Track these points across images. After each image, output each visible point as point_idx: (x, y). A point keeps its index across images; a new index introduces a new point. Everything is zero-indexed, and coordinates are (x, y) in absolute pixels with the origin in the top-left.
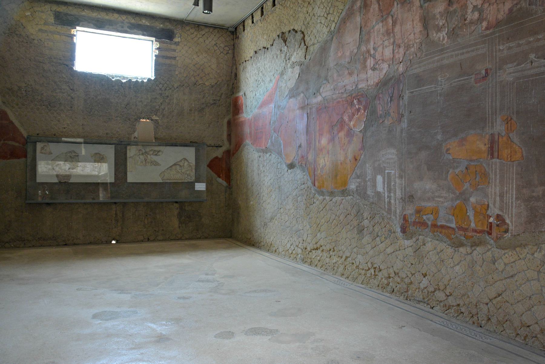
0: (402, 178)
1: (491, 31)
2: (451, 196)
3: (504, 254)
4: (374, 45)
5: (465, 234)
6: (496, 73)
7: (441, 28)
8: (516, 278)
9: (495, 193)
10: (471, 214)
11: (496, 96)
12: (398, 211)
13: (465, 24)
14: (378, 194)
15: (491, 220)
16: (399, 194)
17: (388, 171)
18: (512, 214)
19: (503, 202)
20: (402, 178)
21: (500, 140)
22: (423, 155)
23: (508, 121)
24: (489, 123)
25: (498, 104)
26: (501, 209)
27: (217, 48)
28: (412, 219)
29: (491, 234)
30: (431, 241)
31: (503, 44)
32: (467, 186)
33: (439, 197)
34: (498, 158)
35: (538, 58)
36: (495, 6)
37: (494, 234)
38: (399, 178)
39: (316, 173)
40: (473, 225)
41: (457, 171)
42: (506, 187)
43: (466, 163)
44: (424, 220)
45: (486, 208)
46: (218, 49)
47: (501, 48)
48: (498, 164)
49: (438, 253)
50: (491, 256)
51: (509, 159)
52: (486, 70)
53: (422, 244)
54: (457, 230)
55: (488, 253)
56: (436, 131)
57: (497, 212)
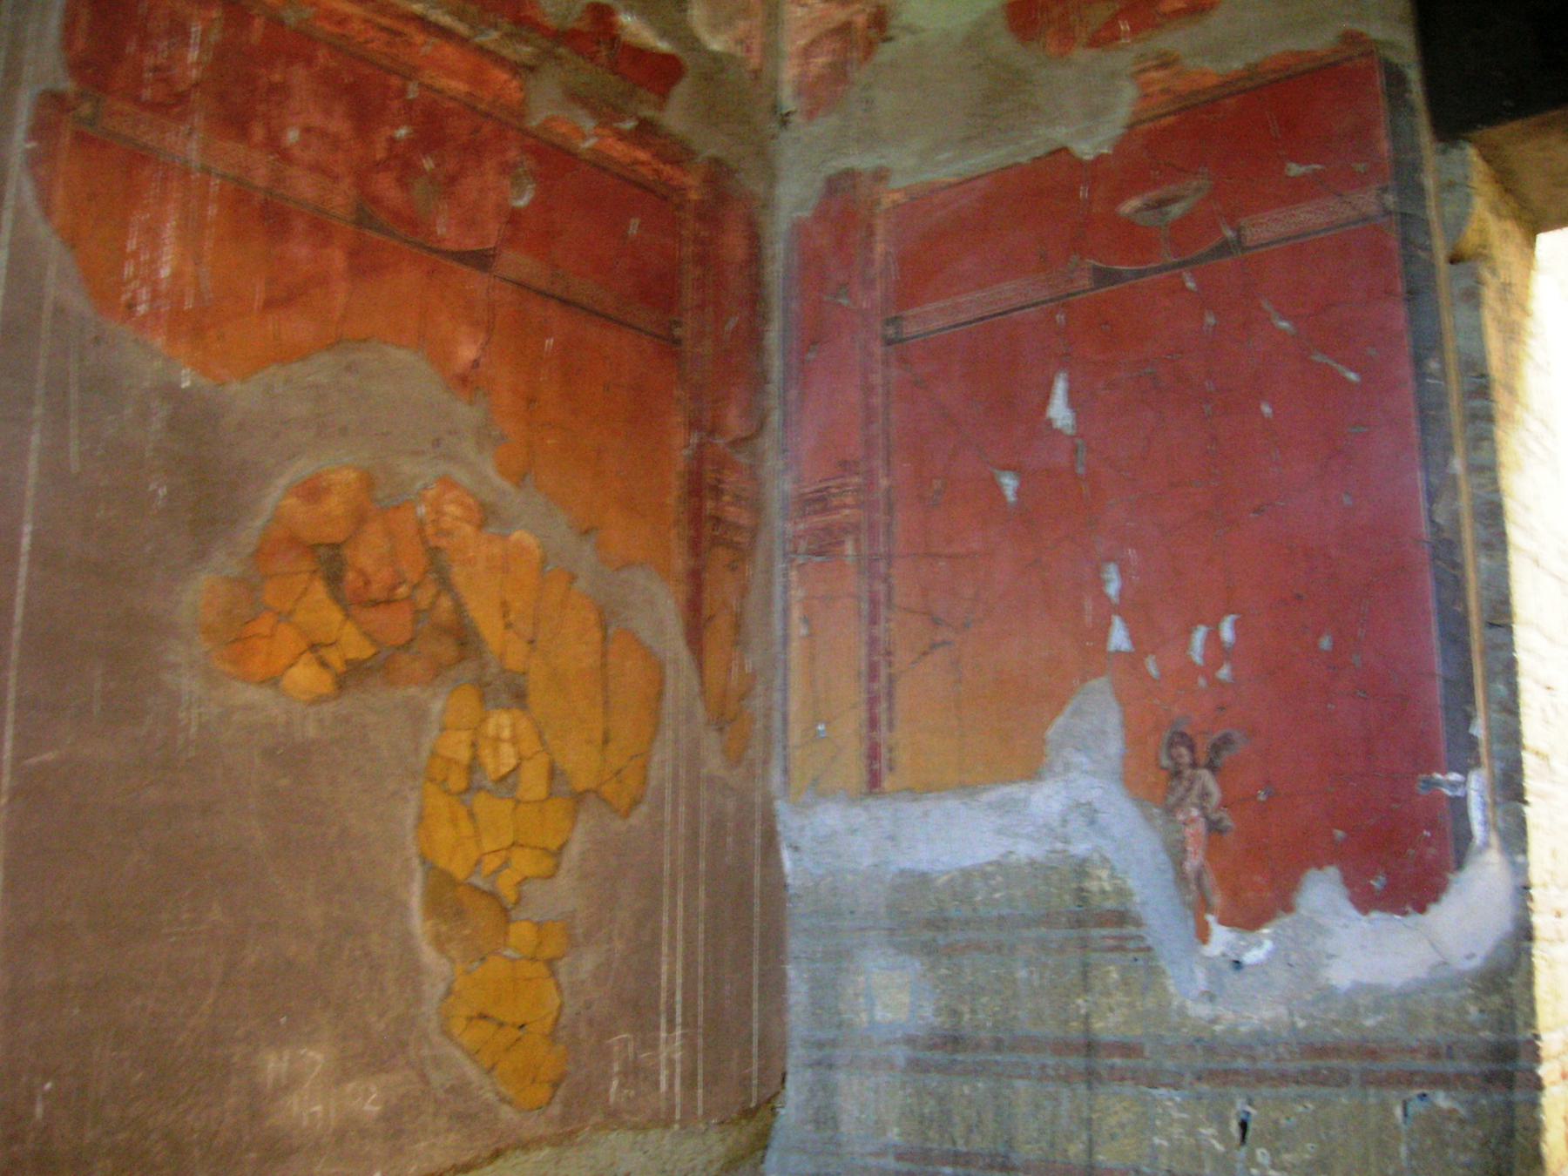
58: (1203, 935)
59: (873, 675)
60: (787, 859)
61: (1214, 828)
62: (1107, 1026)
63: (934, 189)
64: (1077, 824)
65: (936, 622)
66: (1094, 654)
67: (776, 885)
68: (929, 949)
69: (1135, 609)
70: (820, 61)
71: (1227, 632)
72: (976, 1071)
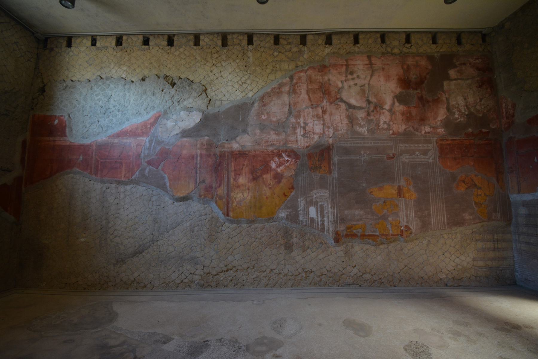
0: (334, 208)
1: (395, 136)
2: (375, 217)
3: (408, 245)
4: (304, 121)
5: (386, 237)
6: (399, 156)
7: (363, 126)
9: (403, 215)
10: (389, 227)
11: (400, 168)
12: (331, 229)
13: (379, 128)
14: (312, 220)
15: (402, 228)
16: (331, 218)
17: (320, 204)
18: (413, 224)
19: (408, 219)
20: (334, 208)
21: (404, 189)
24: (397, 180)
25: (401, 171)
26: (407, 222)
27: (18, 49)
28: (343, 233)
29: (403, 236)
30: (358, 245)
31: (402, 144)
32: (385, 211)
33: (366, 218)
34: (403, 198)
35: (420, 154)
36: (397, 125)
37: (405, 235)
38: (332, 208)
39: (230, 205)
40: (391, 232)
42: (409, 211)
44: (355, 233)
45: (399, 222)
46: (19, 50)
48: (404, 201)
50: (400, 247)
51: (410, 198)
52: (393, 154)
53: (351, 248)
54: (380, 236)
55: (398, 246)
56: (362, 181)
57: (405, 224)
60: (511, 199)
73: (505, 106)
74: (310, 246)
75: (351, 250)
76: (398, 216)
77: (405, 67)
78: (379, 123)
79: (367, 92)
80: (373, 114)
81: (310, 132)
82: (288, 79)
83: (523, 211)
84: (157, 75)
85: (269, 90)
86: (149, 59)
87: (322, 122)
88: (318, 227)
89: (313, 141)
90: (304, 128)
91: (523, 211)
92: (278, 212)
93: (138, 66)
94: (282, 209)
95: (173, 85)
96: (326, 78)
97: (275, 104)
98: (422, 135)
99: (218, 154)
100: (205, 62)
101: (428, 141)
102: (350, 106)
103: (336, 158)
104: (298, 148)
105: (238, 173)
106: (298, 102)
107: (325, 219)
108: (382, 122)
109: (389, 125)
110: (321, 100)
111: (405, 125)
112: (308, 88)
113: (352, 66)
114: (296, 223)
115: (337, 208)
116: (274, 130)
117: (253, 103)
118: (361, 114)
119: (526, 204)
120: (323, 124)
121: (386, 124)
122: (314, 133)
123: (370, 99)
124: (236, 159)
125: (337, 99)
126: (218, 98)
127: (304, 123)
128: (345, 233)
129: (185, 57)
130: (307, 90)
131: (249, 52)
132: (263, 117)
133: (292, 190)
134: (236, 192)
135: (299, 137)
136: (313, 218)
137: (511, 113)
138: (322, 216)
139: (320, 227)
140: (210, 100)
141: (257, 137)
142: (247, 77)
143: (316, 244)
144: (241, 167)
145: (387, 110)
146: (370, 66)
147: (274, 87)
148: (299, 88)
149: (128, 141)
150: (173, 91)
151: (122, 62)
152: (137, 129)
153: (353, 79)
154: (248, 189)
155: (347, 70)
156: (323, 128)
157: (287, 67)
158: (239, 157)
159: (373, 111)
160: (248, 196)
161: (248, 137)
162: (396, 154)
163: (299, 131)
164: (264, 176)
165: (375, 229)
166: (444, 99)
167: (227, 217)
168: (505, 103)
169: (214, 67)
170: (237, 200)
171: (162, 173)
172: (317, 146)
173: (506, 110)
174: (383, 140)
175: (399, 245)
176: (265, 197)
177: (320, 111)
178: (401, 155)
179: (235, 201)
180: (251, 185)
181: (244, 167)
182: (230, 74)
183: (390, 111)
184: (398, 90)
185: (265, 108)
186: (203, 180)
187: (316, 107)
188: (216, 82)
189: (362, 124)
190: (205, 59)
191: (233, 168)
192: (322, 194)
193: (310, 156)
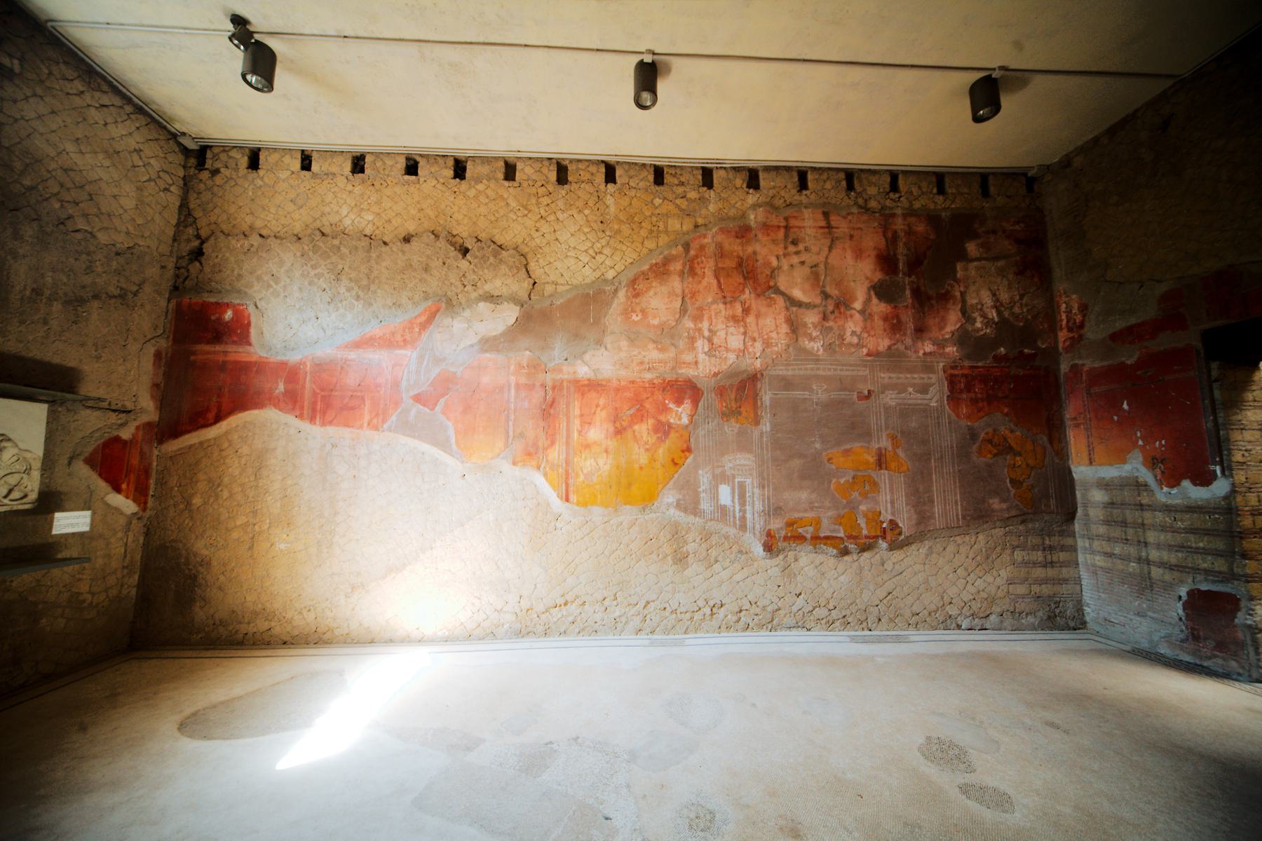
0: (763, 487)
8: (904, 574)
9: (886, 501)
10: (862, 522)
12: (757, 526)
14: (723, 510)
15: (884, 525)
16: (759, 506)
20: (763, 487)
22: (796, 463)
23: (893, 438)
25: (883, 422)
26: (893, 514)
29: (885, 538)
31: (884, 373)
39: (571, 481)
41: (842, 481)
43: (852, 473)
47: (883, 375)
48: (887, 476)
49: (816, 567)
52: (869, 391)
54: (846, 539)
57: (890, 517)
58: (1162, 489)
59: (1089, 446)
60: (1074, 475)
61: (1163, 472)
62: (1145, 501)
63: (1095, 368)
64: (1134, 471)
65: (1102, 439)
66: (1135, 444)
67: (1072, 480)
68: (1105, 489)
69: (1142, 438)
70: (1067, 343)
71: (1163, 442)
72: (1118, 508)
73: (1066, 308)
74: (720, 558)
75: (792, 564)
76: (877, 502)
77: (890, 235)
78: (845, 334)
79: (823, 277)
80: (832, 317)
81: (720, 346)
82: (680, 248)
83: (1098, 496)
84: (433, 232)
85: (646, 267)
86: (418, 202)
87: (742, 330)
88: (735, 523)
89: (725, 364)
90: (710, 340)
91: (1098, 496)
92: (660, 495)
93: (397, 215)
94: (669, 489)
95: (465, 251)
96: (750, 250)
97: (656, 294)
98: (919, 357)
99: (549, 383)
100: (526, 212)
101: (929, 369)
102: (792, 302)
103: (766, 397)
104: (697, 377)
105: (587, 421)
106: (699, 291)
107: (748, 508)
108: (848, 333)
109: (859, 337)
110: (741, 289)
111: (890, 339)
112: (716, 265)
113: (796, 230)
114: (695, 515)
115: (768, 486)
116: (654, 342)
117: (616, 291)
118: (811, 318)
119: (1105, 485)
120: (745, 334)
121: (857, 336)
122: (727, 350)
123: (828, 289)
124: (583, 395)
125: (770, 287)
126: (549, 280)
127: (710, 330)
128: (783, 533)
129: (487, 201)
130: (715, 271)
131: (609, 197)
132: (634, 318)
133: (687, 454)
134: (583, 457)
135: (700, 355)
136: (725, 506)
137: (1077, 321)
138: (743, 503)
139: (737, 522)
140: (535, 283)
141: (623, 355)
142: (604, 242)
143: (731, 554)
144: (593, 411)
145: (858, 312)
146: (827, 230)
147: (654, 261)
148: (701, 265)
149: (377, 357)
150: (464, 264)
151: (365, 206)
152: (393, 334)
153: (797, 253)
154: (606, 451)
155: (786, 236)
156: (744, 340)
157: (678, 226)
158: (589, 391)
159: (833, 312)
160: (605, 464)
161: (606, 353)
162: (873, 391)
163: (701, 345)
164: (636, 427)
165: (837, 527)
166: (958, 294)
167: (567, 503)
168: (1065, 302)
169: (543, 222)
170: (585, 471)
171: (442, 418)
172: (732, 374)
173: (1067, 316)
174: (851, 365)
175: (878, 555)
176: (636, 466)
177: (738, 309)
178: (883, 393)
179: (580, 472)
180: (612, 444)
181: (599, 409)
182: (572, 235)
183: (862, 312)
184: (878, 276)
185: (637, 301)
186: (520, 434)
187: (731, 302)
188: (546, 250)
189: (814, 334)
190: (525, 207)
191: (577, 412)
192: (743, 462)
193: (721, 391)
